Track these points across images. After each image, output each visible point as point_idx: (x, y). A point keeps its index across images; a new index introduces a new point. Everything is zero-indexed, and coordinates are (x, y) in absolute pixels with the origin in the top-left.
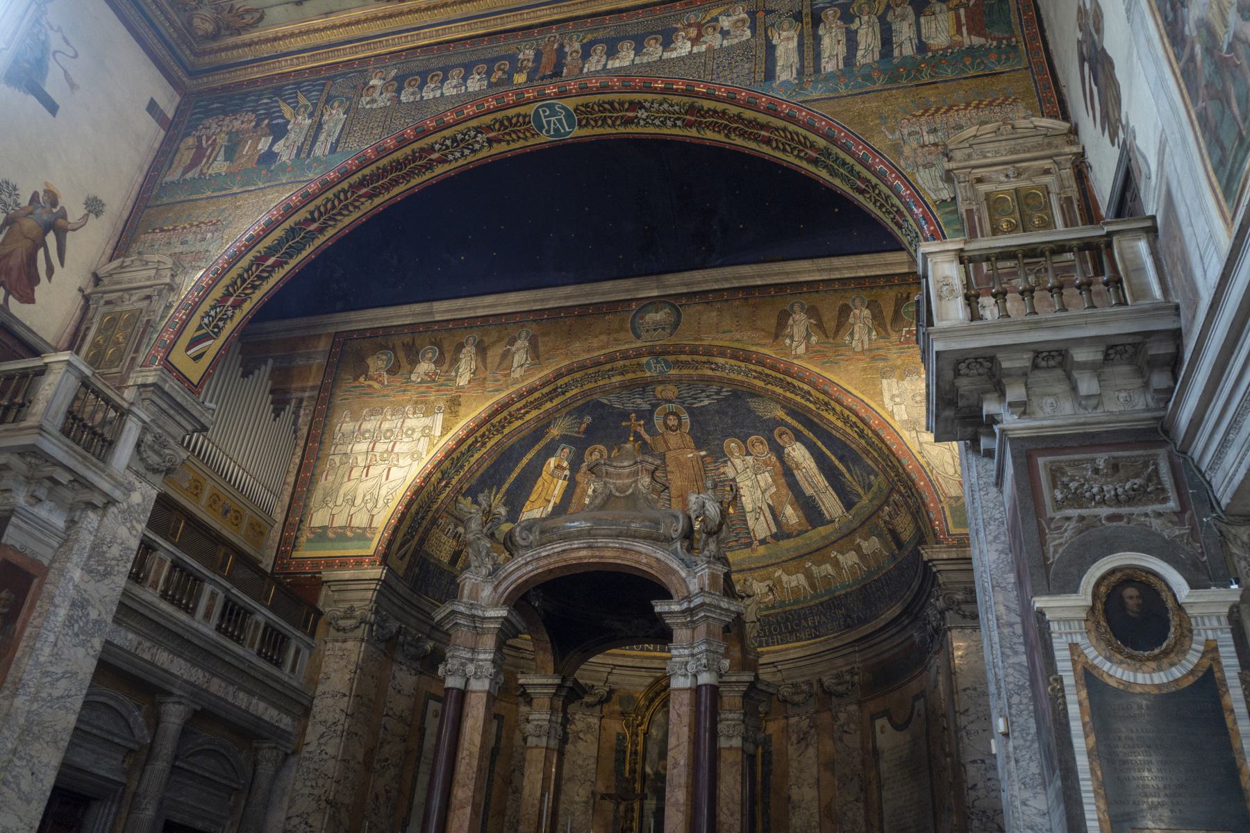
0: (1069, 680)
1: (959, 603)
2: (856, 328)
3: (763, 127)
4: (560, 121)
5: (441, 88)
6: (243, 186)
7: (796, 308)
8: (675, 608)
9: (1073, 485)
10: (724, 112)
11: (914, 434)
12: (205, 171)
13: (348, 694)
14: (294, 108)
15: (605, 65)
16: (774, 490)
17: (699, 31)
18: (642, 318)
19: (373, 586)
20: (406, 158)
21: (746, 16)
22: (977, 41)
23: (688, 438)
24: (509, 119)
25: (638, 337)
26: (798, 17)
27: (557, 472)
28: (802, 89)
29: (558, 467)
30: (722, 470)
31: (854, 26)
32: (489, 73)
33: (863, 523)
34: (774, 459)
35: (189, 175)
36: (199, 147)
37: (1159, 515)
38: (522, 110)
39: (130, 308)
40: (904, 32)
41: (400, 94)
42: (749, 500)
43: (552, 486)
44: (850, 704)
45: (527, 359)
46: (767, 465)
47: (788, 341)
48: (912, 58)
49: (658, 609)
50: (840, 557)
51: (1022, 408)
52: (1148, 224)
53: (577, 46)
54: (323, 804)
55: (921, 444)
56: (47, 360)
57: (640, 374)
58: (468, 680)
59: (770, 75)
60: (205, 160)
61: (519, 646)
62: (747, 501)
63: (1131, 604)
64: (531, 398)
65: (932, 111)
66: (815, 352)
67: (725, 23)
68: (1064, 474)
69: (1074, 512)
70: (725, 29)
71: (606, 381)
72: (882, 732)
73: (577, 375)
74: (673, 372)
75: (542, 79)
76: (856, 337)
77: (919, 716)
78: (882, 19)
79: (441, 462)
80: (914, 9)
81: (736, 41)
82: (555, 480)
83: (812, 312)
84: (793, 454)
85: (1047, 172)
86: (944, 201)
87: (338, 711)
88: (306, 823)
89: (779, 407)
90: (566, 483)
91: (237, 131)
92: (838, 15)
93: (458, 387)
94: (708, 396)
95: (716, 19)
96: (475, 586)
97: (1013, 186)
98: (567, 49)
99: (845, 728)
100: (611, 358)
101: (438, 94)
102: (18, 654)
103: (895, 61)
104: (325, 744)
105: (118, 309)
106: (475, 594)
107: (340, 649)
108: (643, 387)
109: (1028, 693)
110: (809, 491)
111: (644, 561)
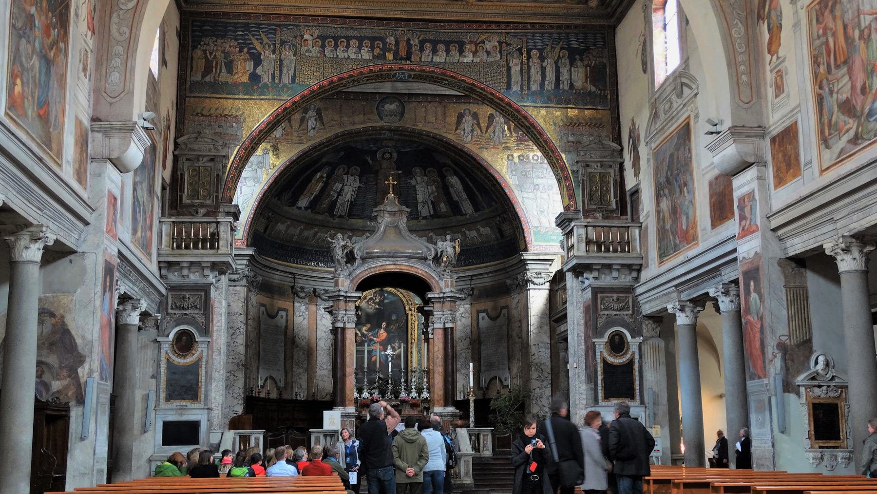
0: (599, 361)
1: (535, 277)
2: (497, 129)
3: (501, 106)
4: (404, 77)
5: (347, 51)
6: (245, 95)
7: (467, 112)
8: (437, 296)
9: (606, 304)
10: (485, 95)
11: (520, 192)
12: (217, 78)
13: (242, 313)
14: (261, 43)
15: (432, 58)
16: (436, 194)
17: (476, 47)
18: (383, 107)
19: (247, 258)
20: (329, 88)
21: (497, 44)
22: (593, 89)
24: (381, 75)
25: (382, 119)
26: (520, 50)
28: (522, 98)
29: (321, 177)
30: (409, 181)
31: (544, 64)
32: (372, 48)
33: (484, 220)
34: (439, 180)
35: (207, 79)
36: (206, 58)
37: (627, 315)
38: (389, 72)
39: (204, 165)
40: (565, 76)
41: (324, 50)
42: (421, 197)
44: (467, 304)
45: (316, 125)
46: (434, 182)
47: (462, 132)
48: (567, 91)
49: (429, 296)
50: (467, 232)
51: (596, 278)
52: (640, 225)
53: (417, 41)
54: (241, 367)
55: (523, 198)
56: (219, 220)
58: (344, 323)
59: (509, 87)
60: (214, 70)
61: (294, 272)
62: (420, 197)
63: (617, 340)
65: (573, 124)
66: (476, 141)
67: (488, 46)
68: (604, 300)
69: (606, 312)
70: (489, 50)
72: (483, 318)
73: (345, 137)
74: (396, 137)
75: (402, 59)
76: (496, 134)
77: (504, 316)
78: (556, 63)
79: (271, 184)
80: (570, 62)
81: (493, 60)
83: (475, 116)
84: (450, 180)
85: (611, 166)
86: (574, 171)
87: (239, 322)
88: (234, 376)
91: (228, 52)
92: (538, 55)
93: (275, 138)
95: (483, 42)
96: (342, 280)
97: (599, 171)
98: (412, 42)
99: (463, 315)
100: (366, 130)
101: (346, 57)
102: (215, 338)
103: (561, 91)
104: (236, 338)
105: (197, 165)
106: (343, 286)
107: (233, 290)
109: (584, 357)
110: (456, 198)
111: (420, 272)
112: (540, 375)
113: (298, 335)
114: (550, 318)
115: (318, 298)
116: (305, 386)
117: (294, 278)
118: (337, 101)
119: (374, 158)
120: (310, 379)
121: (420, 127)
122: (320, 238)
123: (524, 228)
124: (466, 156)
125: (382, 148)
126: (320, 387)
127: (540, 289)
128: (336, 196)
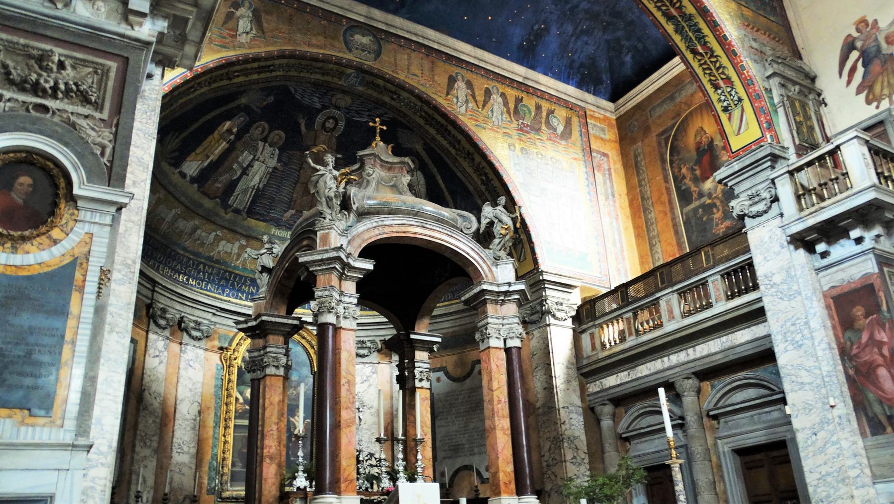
18: (352, 36)
23: (334, 140)
25: (350, 51)
27: (225, 135)
29: (229, 131)
43: (217, 145)
47: (455, 100)
57: (335, 80)
61: (157, 279)
64: (249, 66)
71: (307, 75)
73: (292, 61)
74: (360, 88)
82: (222, 140)
89: (422, 142)
90: (228, 145)
94: (369, 116)
100: (326, 60)
108: (326, 90)
112: (575, 454)
113: (150, 387)
114: (578, 369)
115: (185, 334)
116: (151, 481)
117: (153, 291)
118: (287, 8)
119: (310, 125)
120: (162, 468)
121: (402, 76)
122: (199, 239)
123: (534, 239)
124: (456, 134)
125: (328, 108)
126: (175, 485)
127: (562, 326)
128: (239, 173)
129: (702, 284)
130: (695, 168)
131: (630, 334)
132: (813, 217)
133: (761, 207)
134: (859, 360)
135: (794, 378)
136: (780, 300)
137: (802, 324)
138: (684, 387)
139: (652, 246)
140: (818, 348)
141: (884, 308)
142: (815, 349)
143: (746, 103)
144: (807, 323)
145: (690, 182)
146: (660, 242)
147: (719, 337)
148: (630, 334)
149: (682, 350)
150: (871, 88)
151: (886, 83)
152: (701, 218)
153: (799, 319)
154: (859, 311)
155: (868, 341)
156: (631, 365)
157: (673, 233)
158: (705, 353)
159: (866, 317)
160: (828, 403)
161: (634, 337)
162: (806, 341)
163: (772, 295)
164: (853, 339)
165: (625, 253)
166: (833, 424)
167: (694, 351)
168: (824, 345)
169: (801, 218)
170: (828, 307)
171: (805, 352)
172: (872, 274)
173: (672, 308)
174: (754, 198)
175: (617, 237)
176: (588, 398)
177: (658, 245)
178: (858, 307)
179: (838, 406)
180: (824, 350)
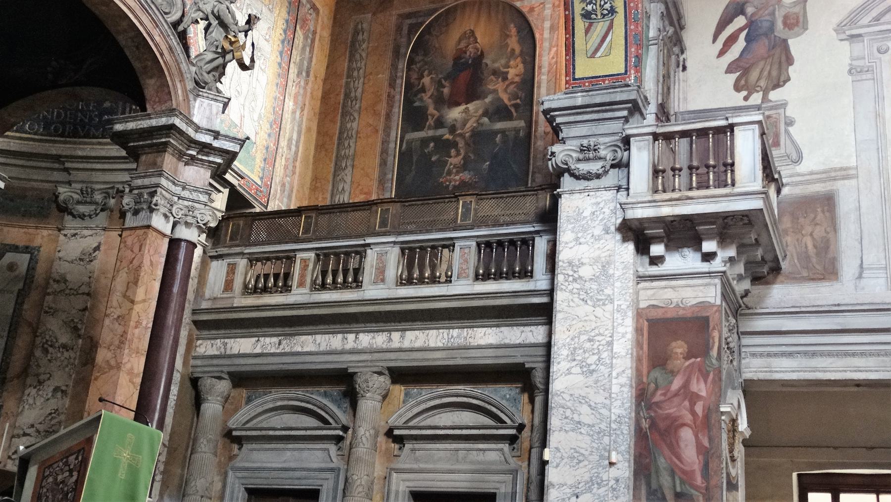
129: (525, 242)
130: (446, 84)
131: (301, 284)
132: (672, 206)
133: (594, 167)
134: (660, 412)
135: (568, 413)
136: (581, 301)
137: (604, 342)
138: (370, 384)
139: (338, 169)
140: (614, 381)
141: (714, 353)
142: (610, 381)
143: (619, 19)
144: (610, 344)
145: (430, 100)
146: (353, 166)
147: (449, 328)
148: (301, 284)
149: (383, 331)
150: (746, 72)
151: (766, 73)
152: (430, 155)
153: (600, 334)
154: (679, 348)
155: (679, 390)
156: (287, 330)
157: (377, 161)
158: (418, 344)
159: (687, 358)
160: (609, 457)
161: (306, 290)
162: (602, 368)
163: (571, 292)
164: (660, 381)
165: (298, 164)
166: (606, 488)
167: (402, 337)
168: (624, 380)
169: (655, 201)
170: (638, 330)
171: (596, 382)
172: (713, 305)
173: (384, 267)
174: (587, 152)
175: (295, 136)
176: (192, 362)
177: (349, 171)
178: (680, 342)
179: (619, 465)
180: (622, 386)
